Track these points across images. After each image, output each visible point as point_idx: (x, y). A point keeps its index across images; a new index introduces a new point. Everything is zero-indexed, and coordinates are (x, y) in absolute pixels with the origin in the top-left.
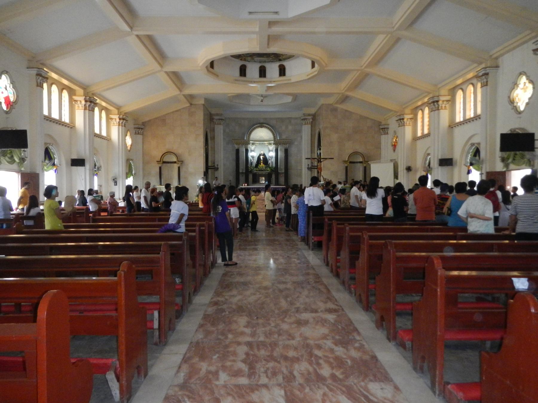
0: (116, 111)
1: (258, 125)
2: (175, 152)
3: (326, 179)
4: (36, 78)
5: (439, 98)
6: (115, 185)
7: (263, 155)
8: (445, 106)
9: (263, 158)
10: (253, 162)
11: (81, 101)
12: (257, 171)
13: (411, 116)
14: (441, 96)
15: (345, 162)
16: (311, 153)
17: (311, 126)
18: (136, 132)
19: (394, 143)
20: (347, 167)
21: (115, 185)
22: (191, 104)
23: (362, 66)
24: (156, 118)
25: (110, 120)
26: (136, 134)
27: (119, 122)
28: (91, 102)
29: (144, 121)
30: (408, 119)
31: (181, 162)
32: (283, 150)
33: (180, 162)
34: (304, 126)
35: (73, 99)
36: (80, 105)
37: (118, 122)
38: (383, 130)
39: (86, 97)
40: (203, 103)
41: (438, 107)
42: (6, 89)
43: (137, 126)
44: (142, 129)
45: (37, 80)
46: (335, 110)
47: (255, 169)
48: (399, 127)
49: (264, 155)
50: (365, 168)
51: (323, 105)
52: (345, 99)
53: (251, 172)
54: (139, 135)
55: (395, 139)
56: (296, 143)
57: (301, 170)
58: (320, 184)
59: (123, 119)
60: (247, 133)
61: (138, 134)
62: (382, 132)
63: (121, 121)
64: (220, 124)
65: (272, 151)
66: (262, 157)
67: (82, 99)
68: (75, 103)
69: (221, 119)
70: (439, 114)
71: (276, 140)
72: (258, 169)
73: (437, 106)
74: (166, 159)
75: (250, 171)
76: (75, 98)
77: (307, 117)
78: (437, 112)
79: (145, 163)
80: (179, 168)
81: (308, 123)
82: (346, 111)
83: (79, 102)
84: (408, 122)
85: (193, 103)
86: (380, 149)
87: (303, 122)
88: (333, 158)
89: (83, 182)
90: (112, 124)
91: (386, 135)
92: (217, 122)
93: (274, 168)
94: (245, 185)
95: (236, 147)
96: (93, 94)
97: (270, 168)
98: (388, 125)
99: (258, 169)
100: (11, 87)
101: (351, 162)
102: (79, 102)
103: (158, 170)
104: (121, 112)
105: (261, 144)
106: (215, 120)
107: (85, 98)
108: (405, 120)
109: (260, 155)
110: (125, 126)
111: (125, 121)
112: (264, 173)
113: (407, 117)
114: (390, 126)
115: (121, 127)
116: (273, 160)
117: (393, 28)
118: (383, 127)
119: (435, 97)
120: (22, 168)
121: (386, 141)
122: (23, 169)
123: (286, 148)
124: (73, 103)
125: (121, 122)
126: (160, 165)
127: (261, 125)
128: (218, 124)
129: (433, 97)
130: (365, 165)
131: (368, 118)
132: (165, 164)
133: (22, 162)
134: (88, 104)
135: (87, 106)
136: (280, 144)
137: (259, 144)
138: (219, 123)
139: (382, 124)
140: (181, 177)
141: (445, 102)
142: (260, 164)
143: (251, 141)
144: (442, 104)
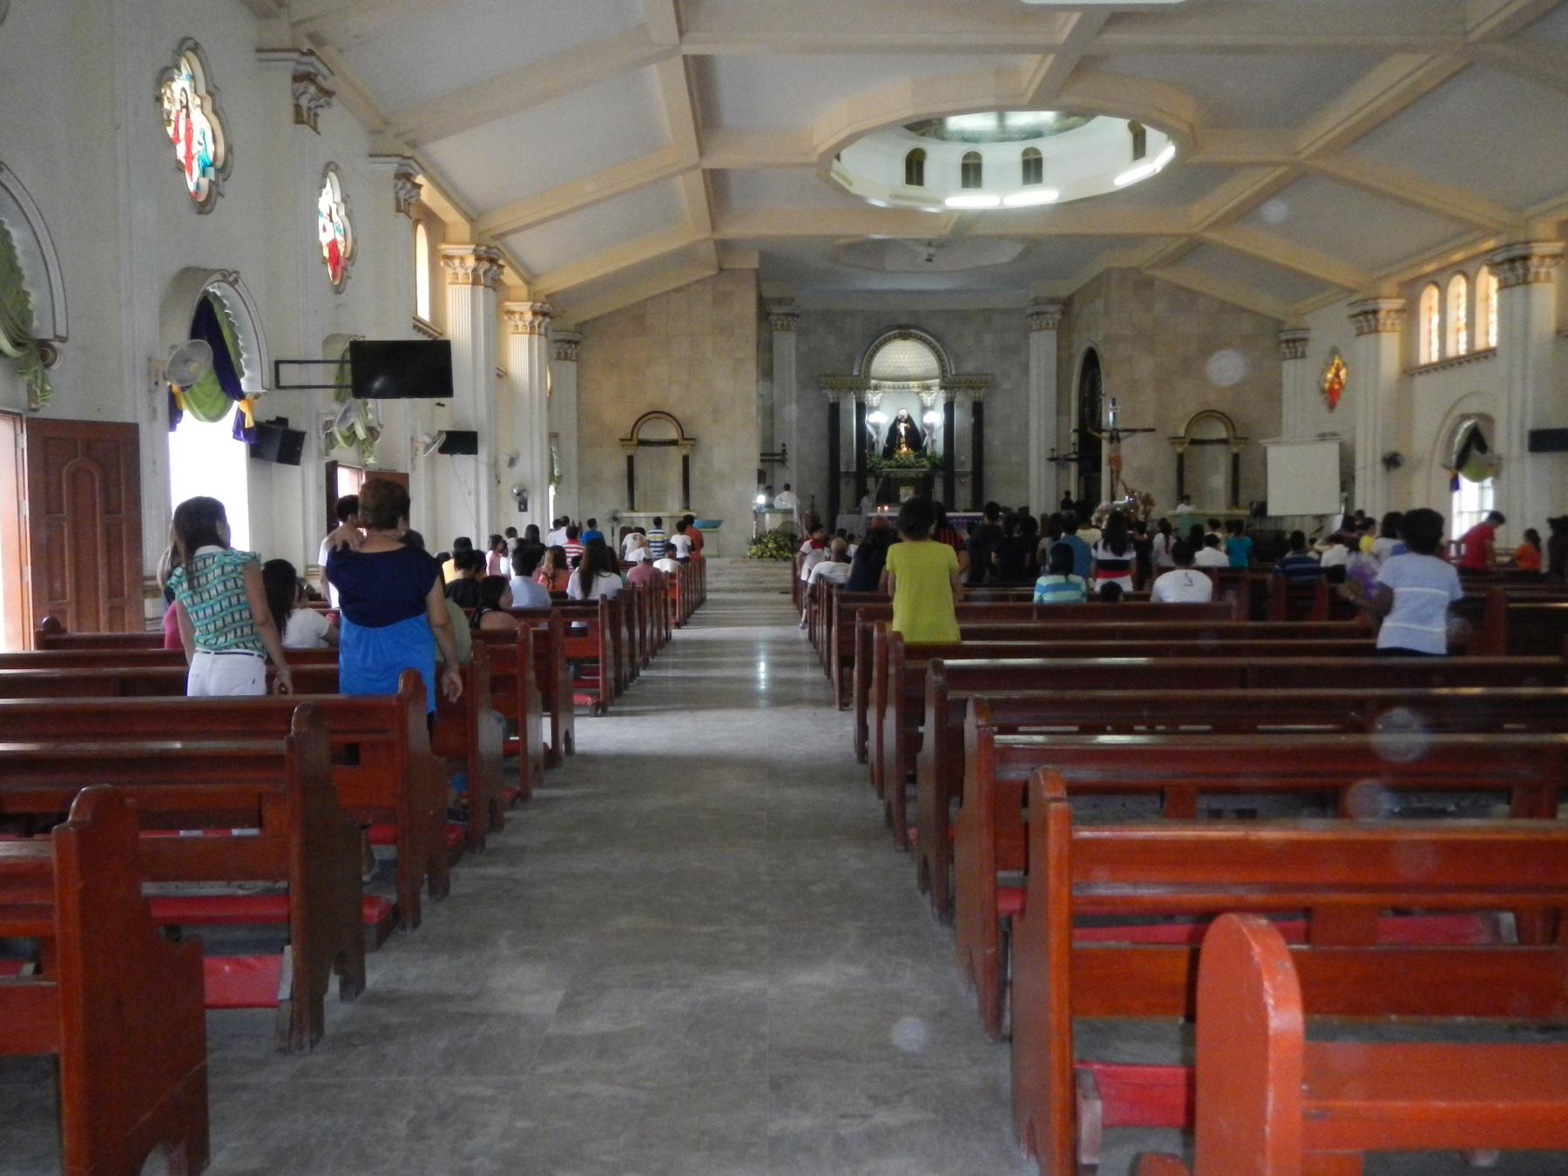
0: (523, 291)
1: (896, 331)
2: (676, 413)
3: (1133, 492)
4: (396, 186)
5: (1530, 248)
6: (520, 510)
7: (906, 422)
8: (1548, 273)
9: (906, 428)
10: (878, 441)
11: (462, 259)
12: (890, 467)
13: (1398, 303)
14: (1537, 241)
15: (1175, 440)
16: (1059, 413)
17: (1058, 333)
18: (559, 353)
19: (1327, 386)
20: (1181, 457)
21: (520, 510)
22: (721, 270)
23: (1297, 153)
24: (617, 312)
25: (506, 318)
26: (558, 358)
27: (532, 323)
28: (492, 261)
29: (581, 319)
30: (1389, 311)
31: (692, 442)
32: (968, 405)
33: (687, 441)
34: (1034, 336)
35: (439, 251)
36: (461, 272)
37: (527, 323)
38: (1291, 345)
39: (478, 245)
40: (756, 265)
41: (1526, 275)
42: (331, 220)
43: (562, 336)
44: (577, 343)
45: (397, 193)
46: (1149, 283)
47: (884, 463)
48: (1358, 335)
49: (909, 420)
50: (1236, 459)
51: (1108, 271)
52: (1192, 249)
53: (871, 470)
54: (568, 362)
55: (1333, 370)
56: (1006, 386)
57: (1025, 465)
58: (1118, 506)
59: (545, 314)
61: (566, 358)
62: (1287, 351)
63: (540, 318)
65: (932, 408)
66: (902, 427)
67: (467, 251)
68: (447, 264)
69: (793, 315)
70: (1527, 296)
71: (949, 376)
73: (1520, 271)
74: (647, 433)
75: (871, 468)
76: (447, 248)
77: (1046, 308)
78: (1519, 290)
79: (585, 445)
80: (686, 460)
81: (1048, 324)
82: (1180, 288)
83: (457, 262)
84: (1389, 322)
85: (724, 267)
86: (1280, 400)
88: (1153, 430)
89: (471, 500)
90: (511, 329)
91: (1300, 362)
92: (779, 323)
94: (883, 511)
95: (831, 396)
96: (494, 238)
97: (929, 459)
98: (1307, 330)
100: (342, 212)
101: (1194, 442)
102: (457, 262)
103: (625, 467)
104: (535, 293)
105: (899, 388)
106: (773, 318)
107: (475, 250)
108: (1382, 315)
109: (897, 421)
110: (546, 335)
111: (548, 320)
112: (912, 473)
113: (1386, 305)
114: (1313, 335)
115: (537, 336)
116: (939, 436)
117: (1466, 33)
118: (1290, 336)
119: (1518, 246)
120: (369, 457)
121: (1300, 380)
122: (371, 461)
123: (977, 399)
124: (442, 263)
125: (536, 323)
126: (630, 452)
127: (905, 331)
129: (1509, 246)
130: (1235, 450)
131: (1244, 310)
132: (641, 448)
133: (370, 439)
134: (485, 265)
135: (481, 272)
136: (959, 388)
137: (894, 388)
139: (1286, 328)
140: (691, 485)
141: (1548, 261)
142: (900, 449)
143: (874, 379)
144: (1538, 267)
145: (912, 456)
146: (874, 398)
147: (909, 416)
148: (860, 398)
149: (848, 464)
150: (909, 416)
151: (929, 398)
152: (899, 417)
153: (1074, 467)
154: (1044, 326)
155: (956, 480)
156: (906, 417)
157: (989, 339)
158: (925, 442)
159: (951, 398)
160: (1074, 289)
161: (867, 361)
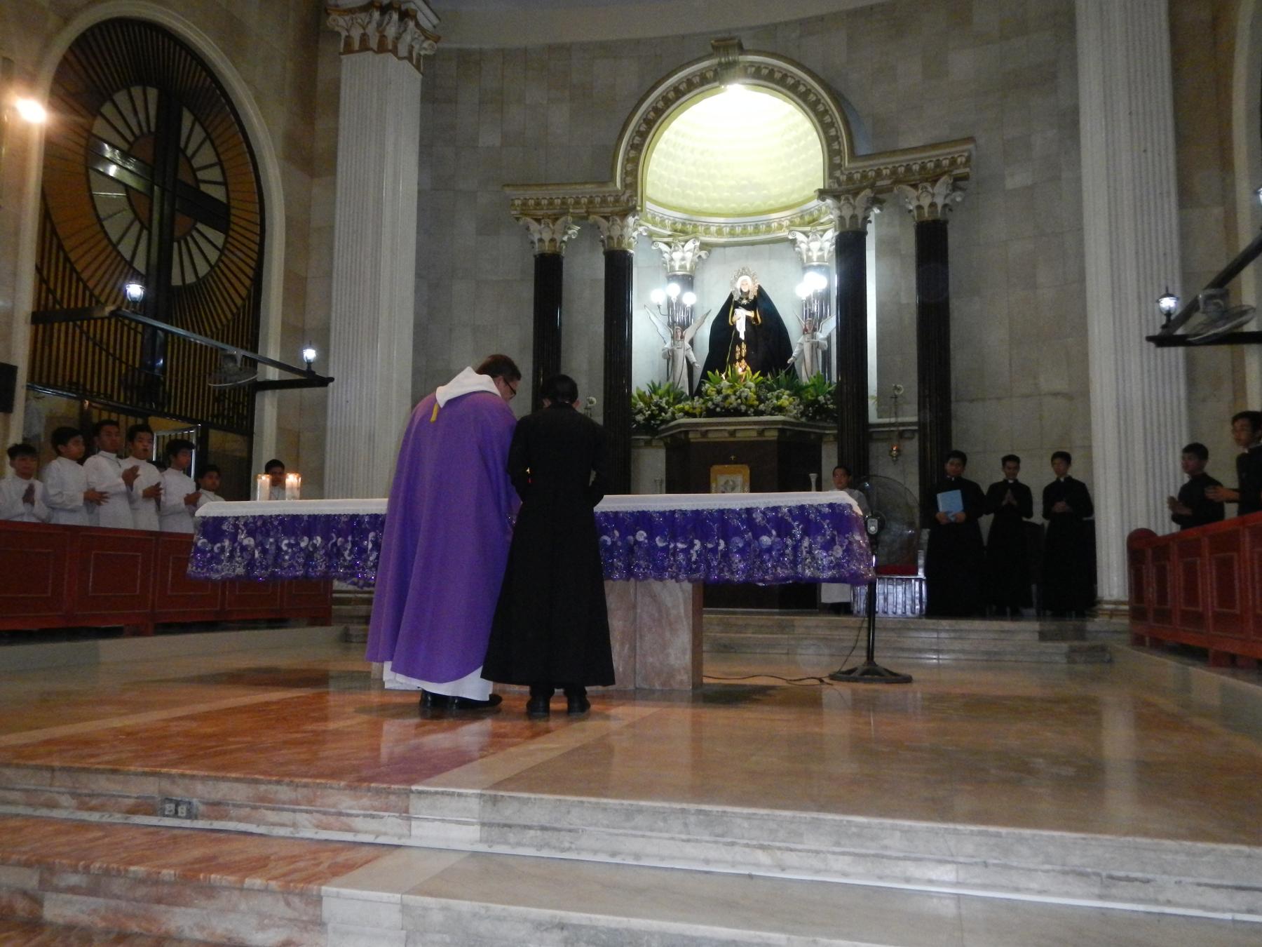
12: (687, 414)
49: (760, 302)
53: (652, 427)
56: (1017, 179)
64: (382, 49)
66: (740, 318)
72: (698, 402)
75: (648, 420)
92: (356, 34)
93: (837, 394)
95: (536, 237)
97: (797, 390)
106: (339, 22)
109: (731, 305)
112: (746, 429)
128: (364, 47)
136: (876, 201)
138: (374, 43)
145: (752, 384)
146: (677, 256)
147: (761, 291)
148: (610, 238)
150: (761, 291)
151: (815, 246)
152: (736, 298)
155: (878, 450)
159: (854, 217)
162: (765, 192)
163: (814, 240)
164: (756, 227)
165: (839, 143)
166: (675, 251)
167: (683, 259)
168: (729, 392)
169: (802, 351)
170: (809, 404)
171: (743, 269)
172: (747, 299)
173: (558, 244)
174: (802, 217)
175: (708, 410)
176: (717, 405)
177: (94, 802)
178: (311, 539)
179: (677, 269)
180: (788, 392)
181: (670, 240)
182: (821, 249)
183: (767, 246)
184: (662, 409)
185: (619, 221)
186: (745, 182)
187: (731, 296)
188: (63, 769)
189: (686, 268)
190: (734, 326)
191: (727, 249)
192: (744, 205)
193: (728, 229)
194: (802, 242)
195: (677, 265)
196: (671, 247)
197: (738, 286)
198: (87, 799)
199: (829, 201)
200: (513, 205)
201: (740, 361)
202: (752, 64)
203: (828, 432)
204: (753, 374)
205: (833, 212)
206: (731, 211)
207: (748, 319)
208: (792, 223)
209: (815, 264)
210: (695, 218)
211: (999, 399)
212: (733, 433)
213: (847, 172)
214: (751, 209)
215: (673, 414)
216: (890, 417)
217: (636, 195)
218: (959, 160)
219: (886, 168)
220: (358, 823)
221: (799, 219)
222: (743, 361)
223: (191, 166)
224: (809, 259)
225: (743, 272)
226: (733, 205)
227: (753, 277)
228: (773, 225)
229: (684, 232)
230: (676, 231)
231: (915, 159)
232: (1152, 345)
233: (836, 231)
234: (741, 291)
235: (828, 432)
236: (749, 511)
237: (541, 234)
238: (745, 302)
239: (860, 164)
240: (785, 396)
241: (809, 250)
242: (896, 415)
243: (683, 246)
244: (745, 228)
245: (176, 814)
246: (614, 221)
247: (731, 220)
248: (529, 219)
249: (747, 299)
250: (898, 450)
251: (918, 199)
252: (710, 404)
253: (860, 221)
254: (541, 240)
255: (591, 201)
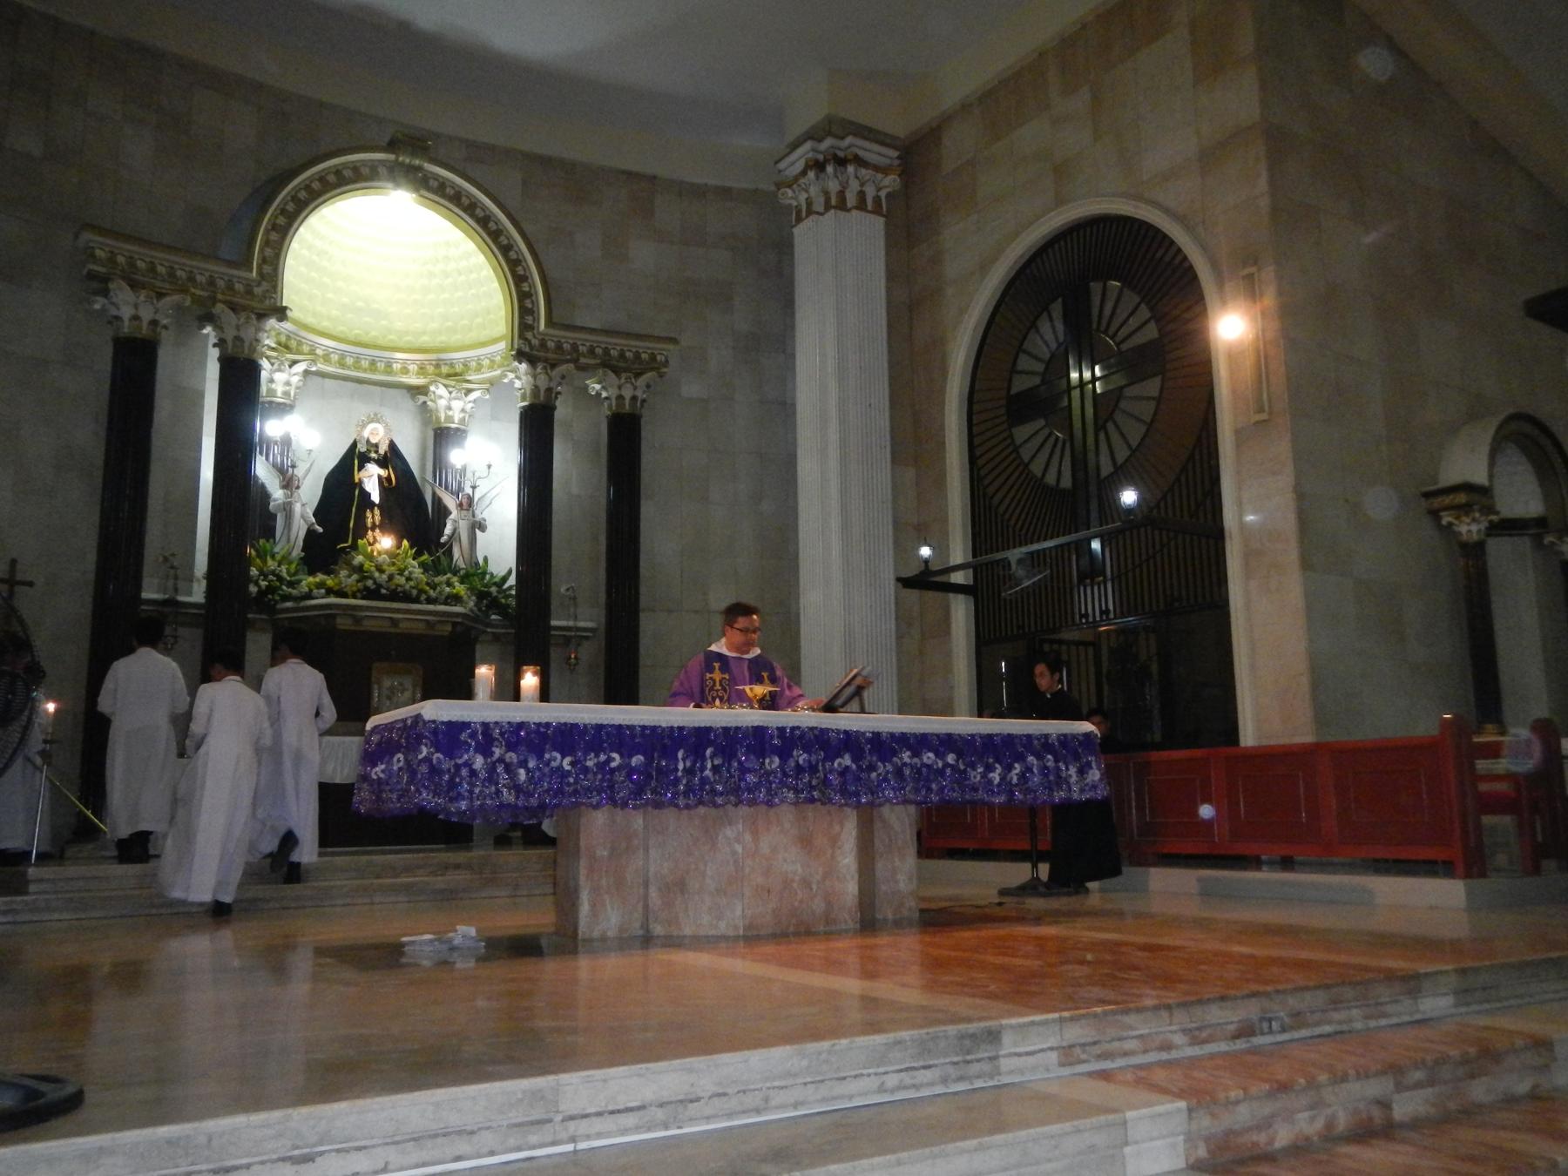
7: (383, 462)
10: (287, 508)
12: (330, 592)
49: (392, 458)
53: (265, 601)
56: (692, 389)
60: (263, 209)
66: (371, 479)
81: (862, 196)
87: (813, 187)
94: (509, 690)
95: (126, 312)
99: (345, 578)
109: (354, 458)
112: (409, 617)
146: (280, 377)
147: (392, 446)
148: (238, 339)
149: (178, 570)
151: (457, 405)
152: (362, 448)
153: (961, 612)
154: (851, 200)
156: (383, 449)
157: (643, 254)
158: (448, 530)
159: (549, 390)
160: (951, 98)
161: (274, 227)
162: (384, 322)
163: (455, 399)
164: (373, 363)
165: (533, 302)
166: (279, 370)
167: (288, 383)
168: (393, 569)
169: (455, 530)
170: (481, 595)
171: (376, 415)
172: (376, 452)
173: (159, 329)
174: (438, 366)
175: (366, 588)
176: (379, 586)
177: (1204, 1035)
178: (597, 756)
179: (279, 394)
180: (455, 579)
181: (274, 354)
182: (463, 410)
183: (378, 388)
184: (280, 578)
185: (255, 322)
186: (360, 304)
187: (354, 445)
188: (1179, 1005)
189: (289, 395)
190: (361, 482)
191: (327, 380)
192: (357, 331)
193: (337, 357)
194: (441, 397)
195: (279, 389)
196: (272, 364)
197: (366, 434)
198: (1197, 1033)
199: (524, 367)
200: (93, 256)
201: (373, 529)
202: (436, 177)
203: (489, 630)
204: (412, 547)
205: (524, 378)
206: (342, 336)
207: (380, 477)
208: (422, 370)
209: (453, 426)
210: (303, 333)
211: (670, 611)
212: (394, 622)
213: (540, 337)
214: (365, 339)
215: (311, 590)
216: (568, 620)
217: (275, 292)
218: (659, 358)
219: (583, 345)
220: (1389, 1008)
221: (432, 368)
222: (377, 531)
223: (1047, 368)
224: (449, 419)
225: (376, 419)
226: (342, 328)
227: (388, 429)
228: (394, 365)
229: (287, 347)
230: (279, 344)
231: (616, 344)
232: (900, 585)
233: (523, 398)
234: (368, 441)
235: (489, 630)
236: (1029, 737)
237: (136, 306)
238: (373, 455)
239: (551, 331)
240: (457, 584)
241: (449, 408)
242: (576, 618)
243: (290, 366)
244: (358, 360)
245: (1271, 1032)
246: (248, 318)
247: (343, 346)
248: (123, 284)
249: (376, 452)
250: (576, 658)
251: (620, 387)
252: (370, 583)
253: (553, 395)
254: (136, 318)
255: (212, 282)
